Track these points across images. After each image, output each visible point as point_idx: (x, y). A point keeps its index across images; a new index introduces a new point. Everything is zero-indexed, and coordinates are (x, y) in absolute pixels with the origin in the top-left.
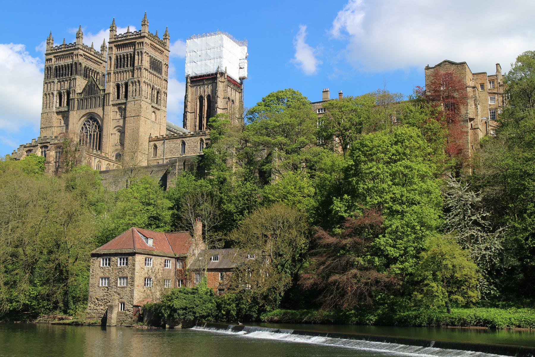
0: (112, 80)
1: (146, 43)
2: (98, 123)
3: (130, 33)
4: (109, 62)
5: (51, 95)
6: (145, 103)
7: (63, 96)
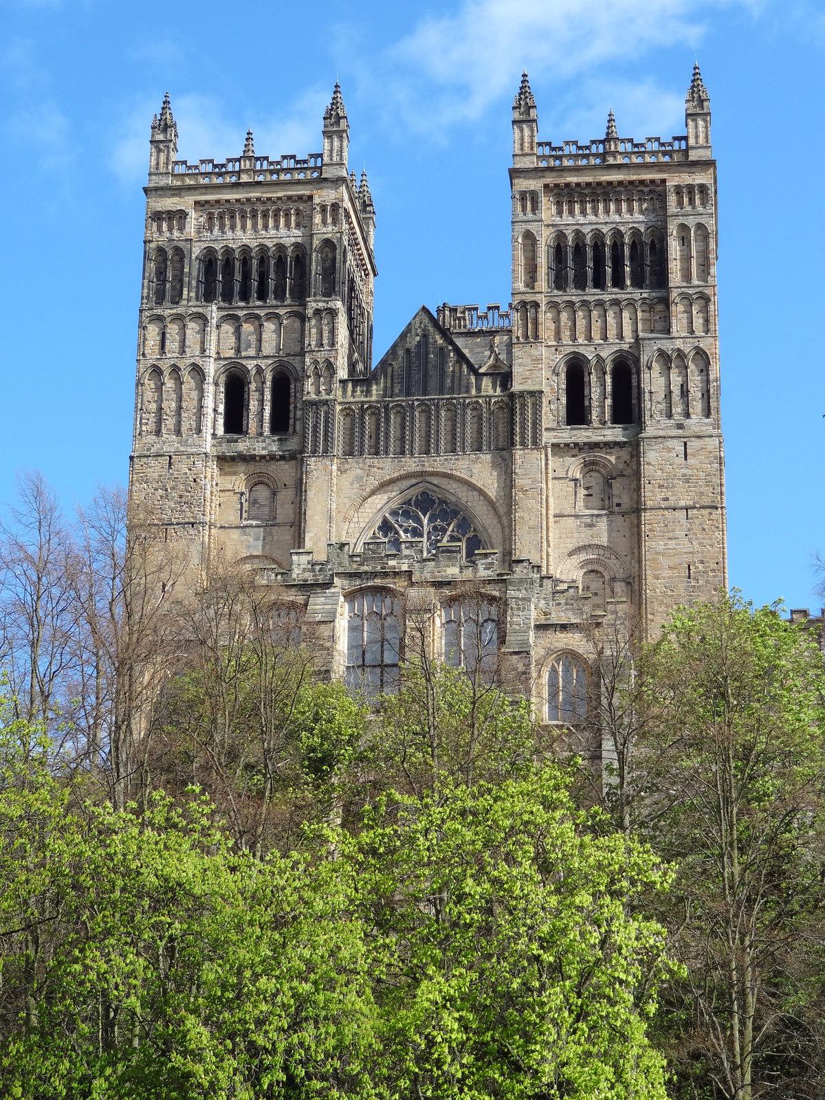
2: (465, 524)
3: (623, 141)
7: (253, 386)
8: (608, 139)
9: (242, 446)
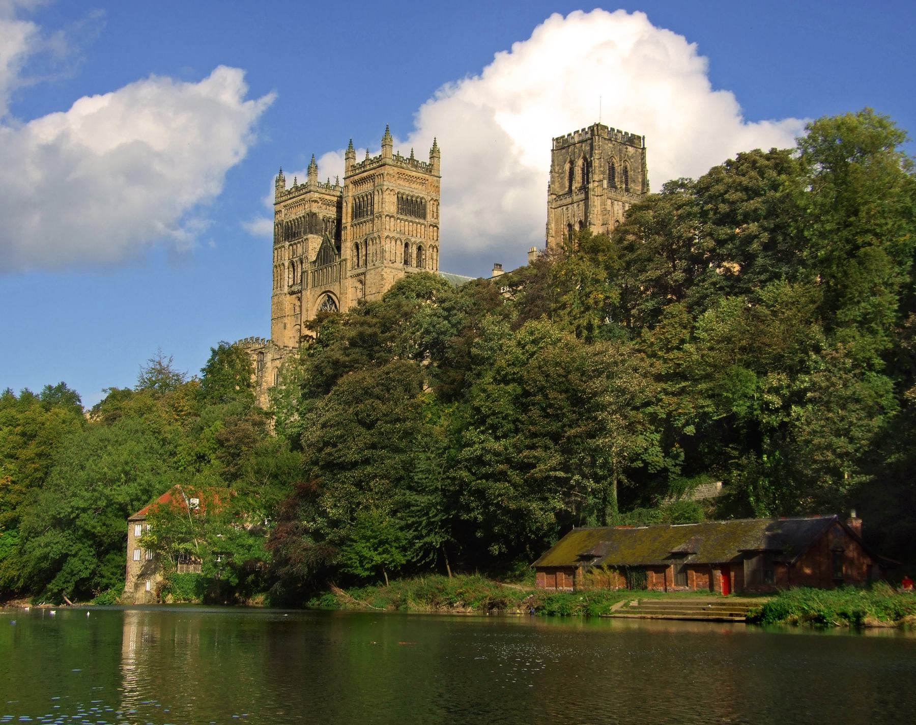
1: (388, 174)
5: (282, 267)
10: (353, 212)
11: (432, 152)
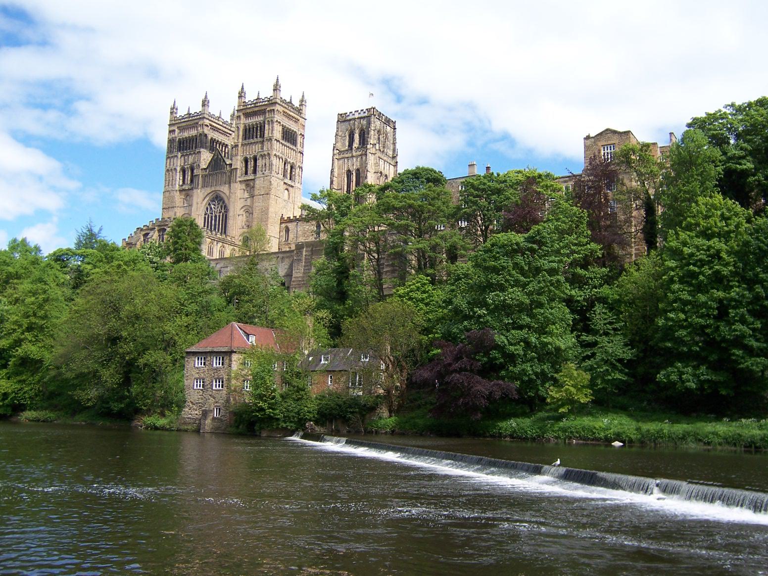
0: (239, 153)
2: (224, 202)
4: (236, 132)
5: (174, 172)
6: (276, 179)
8: (258, 99)
9: (184, 187)
10: (243, 135)
11: (302, 101)
